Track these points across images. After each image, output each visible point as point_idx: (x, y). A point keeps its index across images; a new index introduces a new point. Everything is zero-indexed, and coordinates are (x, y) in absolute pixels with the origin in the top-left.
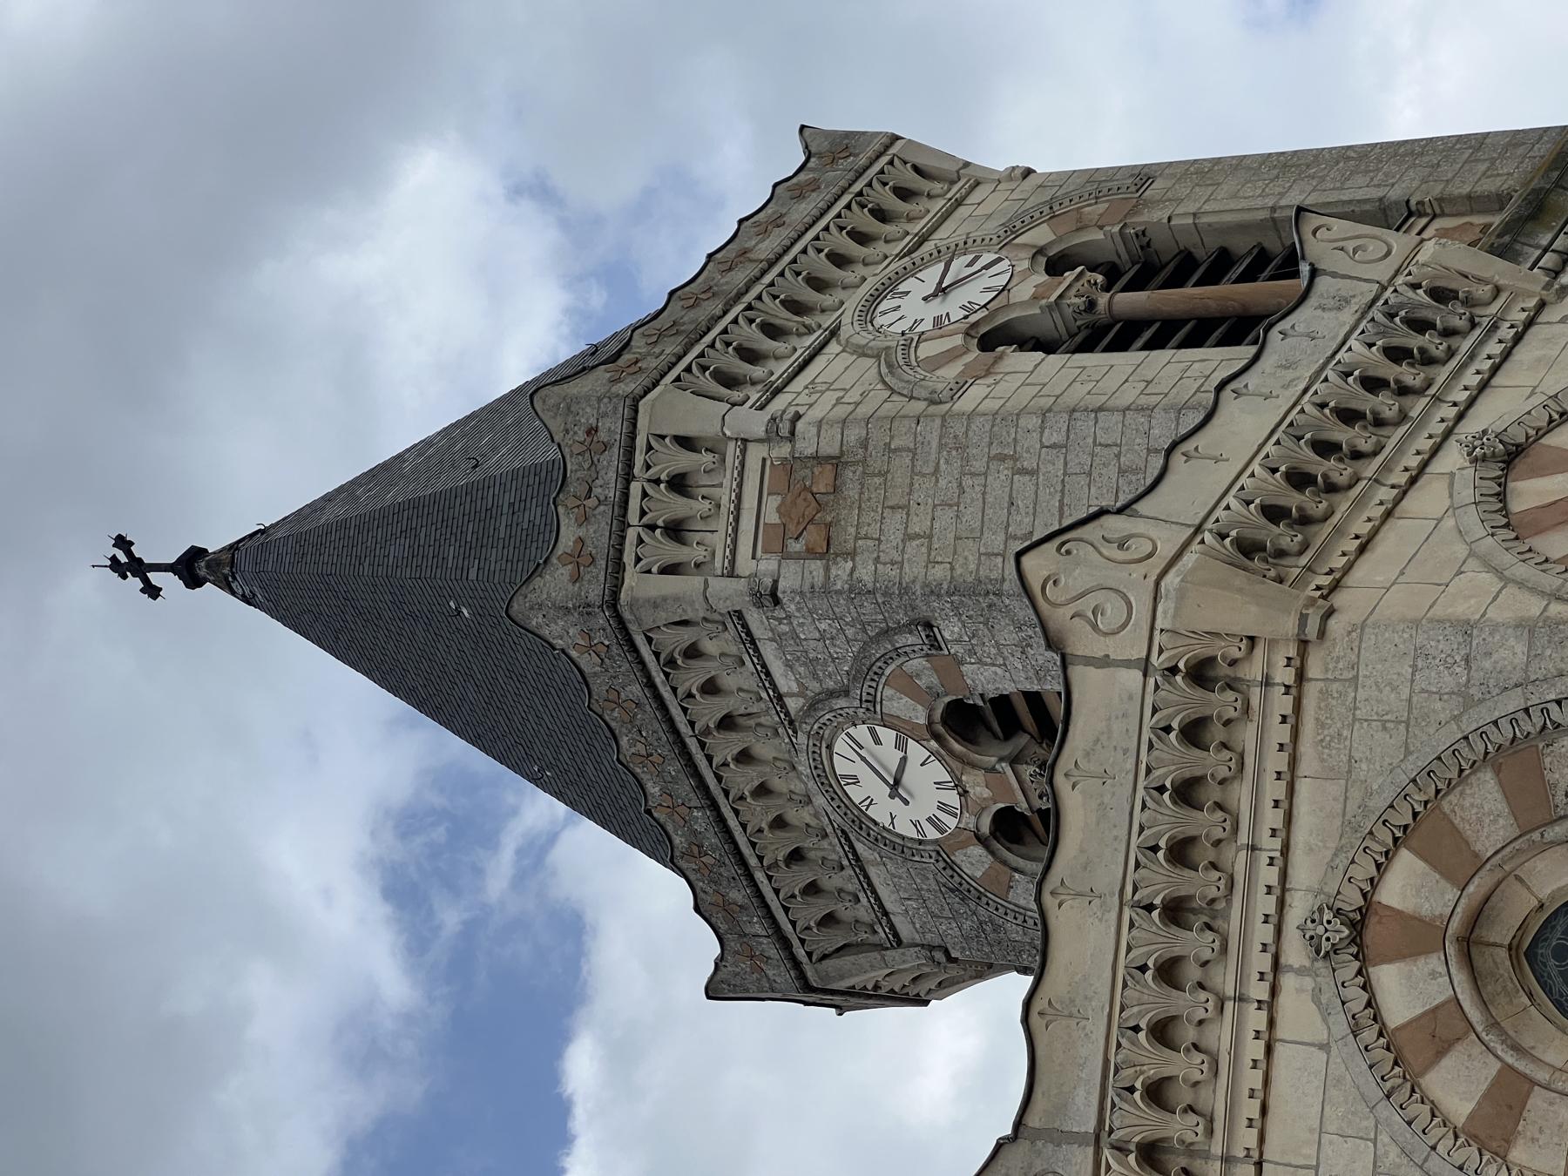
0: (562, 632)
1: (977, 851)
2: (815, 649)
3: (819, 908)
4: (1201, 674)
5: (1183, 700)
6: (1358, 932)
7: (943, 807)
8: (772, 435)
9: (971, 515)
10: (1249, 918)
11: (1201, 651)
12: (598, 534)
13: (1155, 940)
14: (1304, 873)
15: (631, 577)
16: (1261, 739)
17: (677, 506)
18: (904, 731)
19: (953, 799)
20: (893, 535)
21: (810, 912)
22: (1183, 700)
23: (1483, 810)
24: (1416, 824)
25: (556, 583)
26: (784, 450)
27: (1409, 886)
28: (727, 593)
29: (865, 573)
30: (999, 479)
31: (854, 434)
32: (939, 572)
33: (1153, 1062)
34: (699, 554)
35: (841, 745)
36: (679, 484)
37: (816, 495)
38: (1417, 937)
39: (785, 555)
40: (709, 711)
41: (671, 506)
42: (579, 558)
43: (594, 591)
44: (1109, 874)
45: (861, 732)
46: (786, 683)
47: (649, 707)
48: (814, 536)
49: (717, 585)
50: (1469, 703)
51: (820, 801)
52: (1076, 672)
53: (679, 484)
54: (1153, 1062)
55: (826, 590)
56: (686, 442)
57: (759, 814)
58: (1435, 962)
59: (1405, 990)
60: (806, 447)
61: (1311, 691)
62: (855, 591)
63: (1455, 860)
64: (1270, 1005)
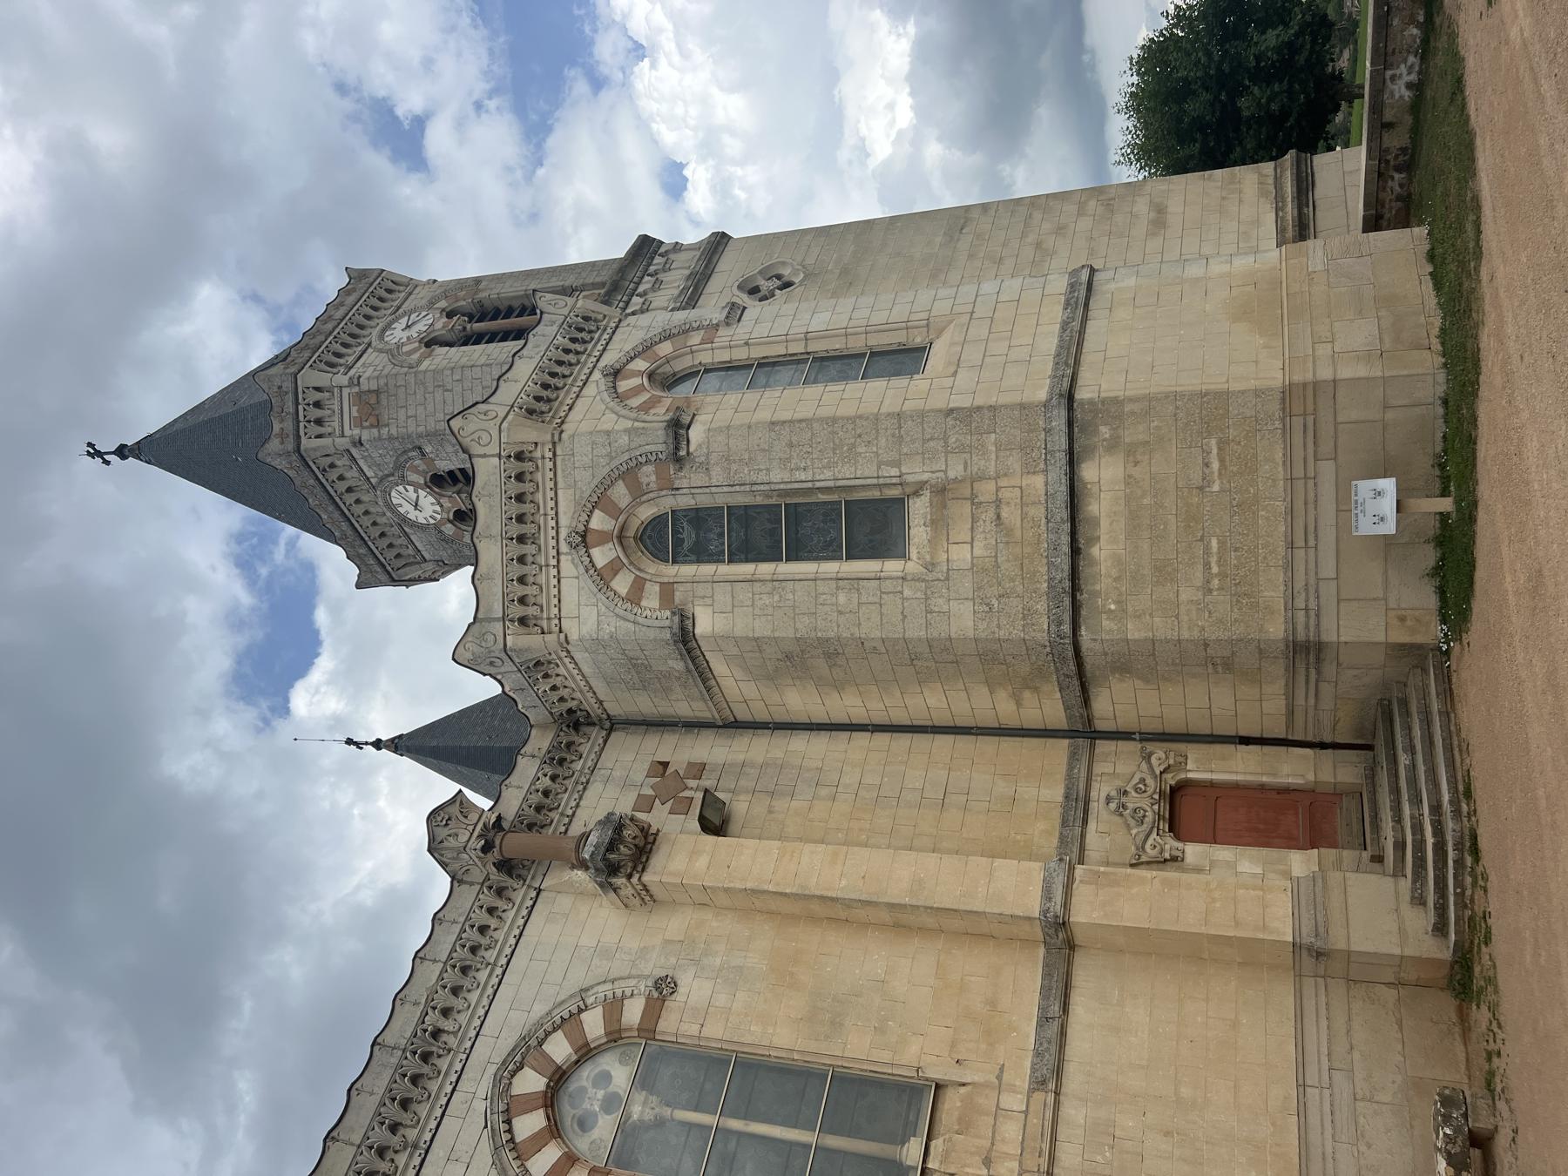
0: (280, 463)
2: (378, 460)
3: (394, 552)
4: (520, 457)
5: (515, 467)
6: (584, 539)
8: (351, 384)
9: (430, 408)
10: (547, 539)
11: (519, 449)
12: (289, 425)
13: (516, 550)
14: (564, 521)
15: (304, 440)
16: (544, 477)
17: (318, 413)
18: (417, 486)
19: (438, 508)
20: (402, 416)
21: (391, 554)
22: (515, 467)
24: (600, 501)
25: (274, 445)
26: (356, 389)
27: (599, 521)
28: (342, 443)
29: (394, 431)
30: (439, 395)
31: (382, 382)
32: (421, 429)
33: (520, 590)
34: (330, 430)
35: (393, 494)
36: (317, 405)
37: (371, 404)
38: (604, 538)
39: (363, 428)
40: (342, 486)
41: (315, 413)
42: (282, 436)
43: (290, 446)
44: (496, 530)
45: (400, 488)
46: (370, 473)
47: (318, 489)
48: (372, 420)
49: (338, 440)
50: (612, 459)
52: (475, 460)
53: (317, 405)
54: (520, 590)
55: (380, 439)
56: (318, 389)
57: (366, 521)
58: (610, 545)
59: (602, 555)
60: (365, 387)
61: (559, 460)
62: (391, 438)
63: (613, 511)
64: (558, 566)
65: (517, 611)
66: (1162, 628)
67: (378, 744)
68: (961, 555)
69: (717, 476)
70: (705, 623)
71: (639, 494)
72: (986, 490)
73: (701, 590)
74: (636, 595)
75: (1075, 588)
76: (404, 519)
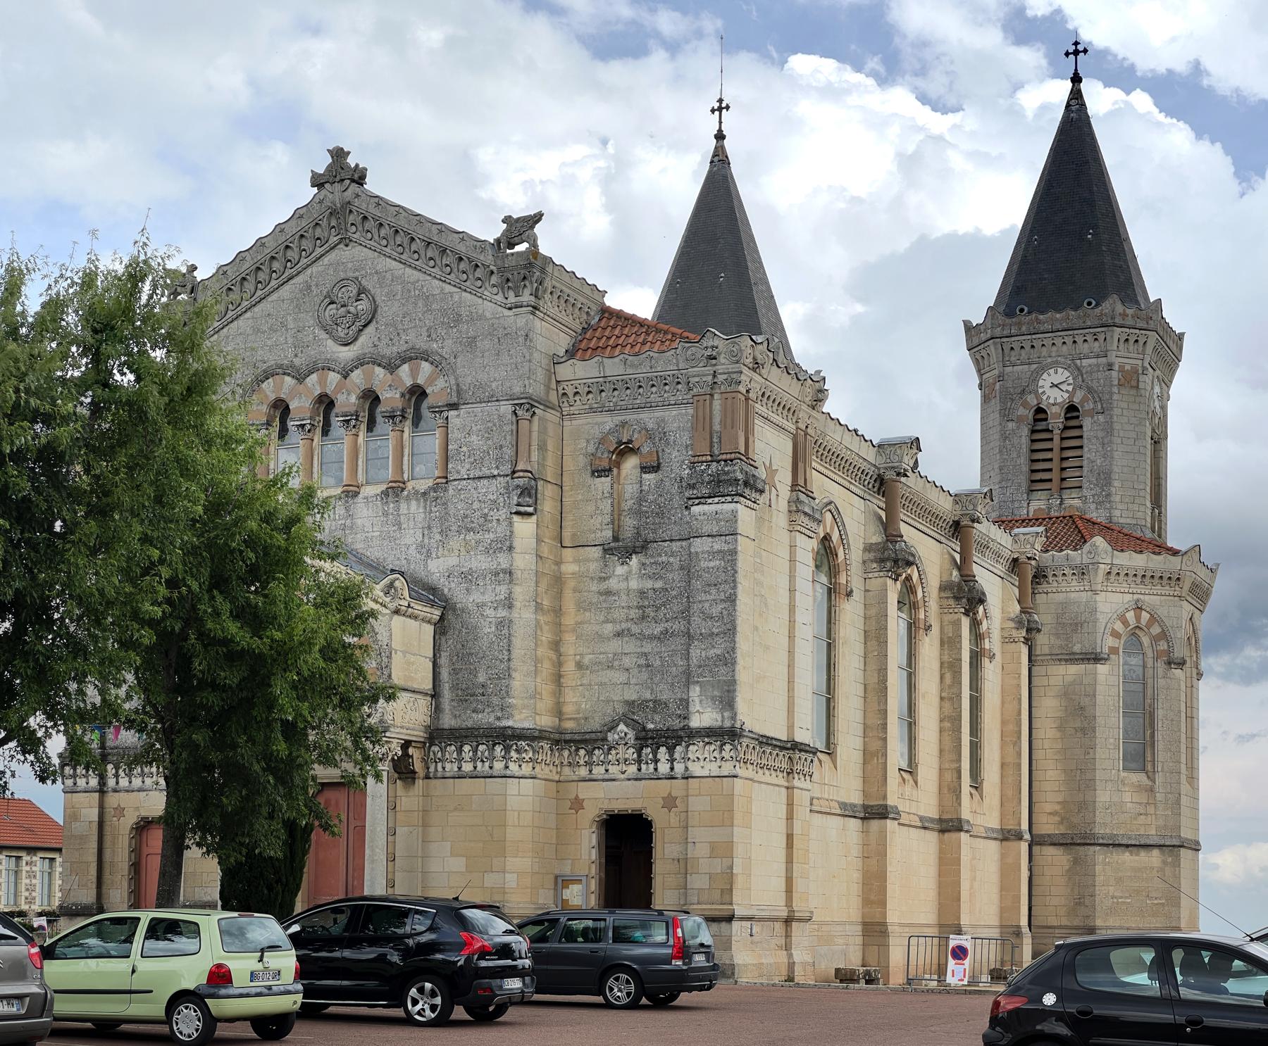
1: (1036, 402)
2: (1095, 375)
6: (1139, 609)
7: (1049, 397)
10: (1142, 589)
13: (1141, 573)
14: (1147, 597)
16: (1167, 590)
18: (1072, 394)
19: (1052, 401)
23: (1156, 630)
24: (1153, 619)
27: (1145, 616)
29: (1115, 397)
30: (1133, 435)
35: (1067, 374)
38: (1138, 618)
44: (1151, 565)
51: (1049, 360)
54: (1122, 574)
57: (1048, 342)
59: (1130, 616)
62: (1111, 393)
63: (1149, 625)
65: (1115, 571)
66: (1100, 879)
67: (720, 136)
68: (1127, 797)
69: (1162, 682)
70: (1102, 669)
71: (1155, 639)
72: (1151, 810)
73: (1116, 668)
74: (1115, 634)
75: (1114, 845)
76: (1043, 369)
